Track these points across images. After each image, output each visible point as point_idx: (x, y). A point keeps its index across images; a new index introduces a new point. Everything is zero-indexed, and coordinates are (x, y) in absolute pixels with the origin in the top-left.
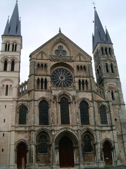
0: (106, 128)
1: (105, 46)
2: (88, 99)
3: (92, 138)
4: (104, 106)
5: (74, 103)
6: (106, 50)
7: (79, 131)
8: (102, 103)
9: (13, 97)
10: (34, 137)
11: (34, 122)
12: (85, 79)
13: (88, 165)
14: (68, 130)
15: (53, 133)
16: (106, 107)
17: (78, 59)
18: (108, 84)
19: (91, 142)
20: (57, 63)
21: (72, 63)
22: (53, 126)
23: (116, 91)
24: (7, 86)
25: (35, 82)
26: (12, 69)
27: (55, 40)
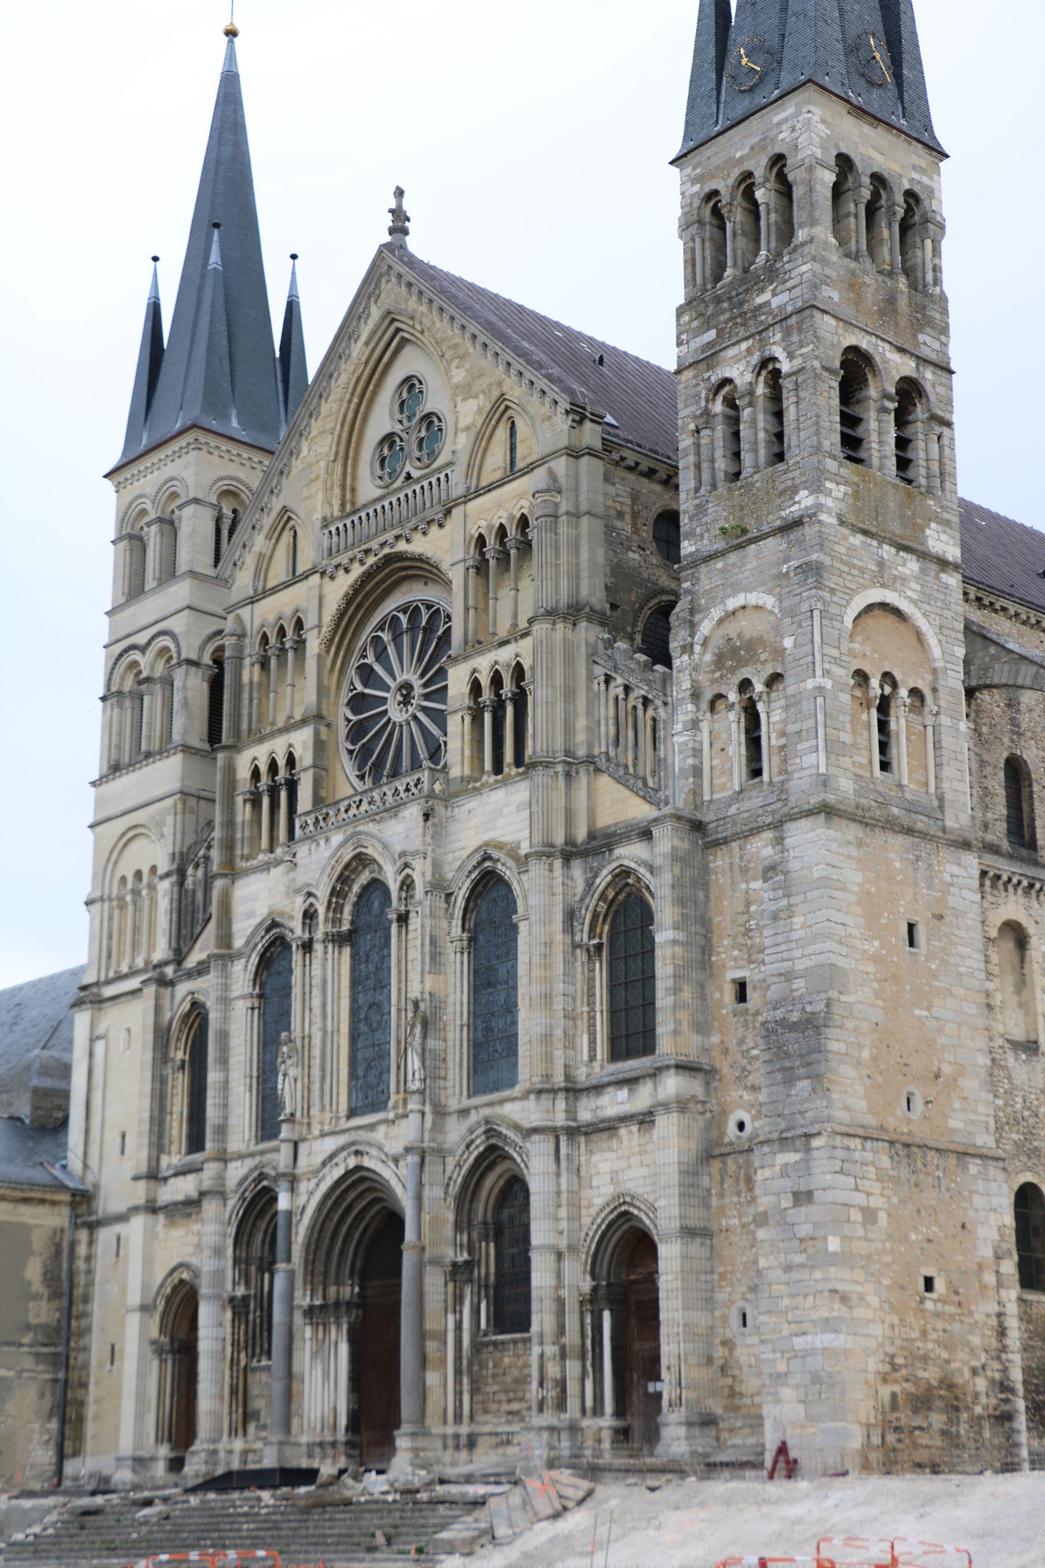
0: (623, 1094)
2: (512, 852)
13: (500, 1451)
14: (366, 1162)
20: (367, 576)
21: (449, 525)
25: (239, 800)
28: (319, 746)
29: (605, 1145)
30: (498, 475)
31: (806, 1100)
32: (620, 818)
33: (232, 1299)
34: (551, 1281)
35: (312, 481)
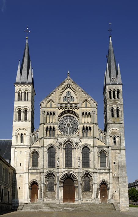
0: (104, 170)
1: (113, 88)
2: (90, 145)
3: (91, 179)
4: (104, 151)
5: (77, 149)
6: (114, 92)
7: (79, 173)
8: (103, 148)
9: (27, 144)
10: (43, 178)
11: (43, 166)
12: (88, 125)
14: (70, 172)
15: (58, 175)
17: (84, 105)
18: (111, 130)
19: (90, 182)
22: (58, 169)
23: (117, 136)
24: (22, 134)
25: (45, 130)
26: (26, 119)
30: (84, 107)
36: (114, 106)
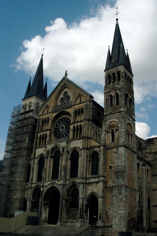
0: (93, 179)
4: (97, 152)
8: (94, 149)
13: (71, 223)
14: (55, 185)
15: (42, 189)
16: (98, 154)
21: (71, 109)
25: (38, 139)
27: (59, 87)
28: (50, 133)
29: (90, 185)
30: (78, 103)
31: (121, 181)
32: (94, 145)
33: (32, 202)
34: (82, 202)
35: (52, 102)
36: (112, 93)
